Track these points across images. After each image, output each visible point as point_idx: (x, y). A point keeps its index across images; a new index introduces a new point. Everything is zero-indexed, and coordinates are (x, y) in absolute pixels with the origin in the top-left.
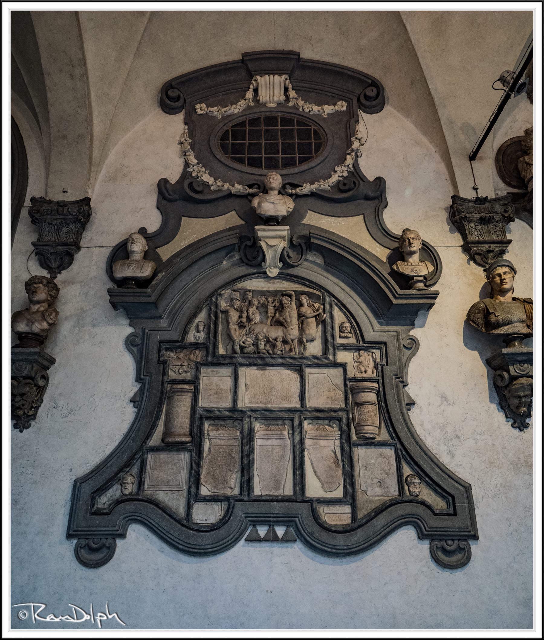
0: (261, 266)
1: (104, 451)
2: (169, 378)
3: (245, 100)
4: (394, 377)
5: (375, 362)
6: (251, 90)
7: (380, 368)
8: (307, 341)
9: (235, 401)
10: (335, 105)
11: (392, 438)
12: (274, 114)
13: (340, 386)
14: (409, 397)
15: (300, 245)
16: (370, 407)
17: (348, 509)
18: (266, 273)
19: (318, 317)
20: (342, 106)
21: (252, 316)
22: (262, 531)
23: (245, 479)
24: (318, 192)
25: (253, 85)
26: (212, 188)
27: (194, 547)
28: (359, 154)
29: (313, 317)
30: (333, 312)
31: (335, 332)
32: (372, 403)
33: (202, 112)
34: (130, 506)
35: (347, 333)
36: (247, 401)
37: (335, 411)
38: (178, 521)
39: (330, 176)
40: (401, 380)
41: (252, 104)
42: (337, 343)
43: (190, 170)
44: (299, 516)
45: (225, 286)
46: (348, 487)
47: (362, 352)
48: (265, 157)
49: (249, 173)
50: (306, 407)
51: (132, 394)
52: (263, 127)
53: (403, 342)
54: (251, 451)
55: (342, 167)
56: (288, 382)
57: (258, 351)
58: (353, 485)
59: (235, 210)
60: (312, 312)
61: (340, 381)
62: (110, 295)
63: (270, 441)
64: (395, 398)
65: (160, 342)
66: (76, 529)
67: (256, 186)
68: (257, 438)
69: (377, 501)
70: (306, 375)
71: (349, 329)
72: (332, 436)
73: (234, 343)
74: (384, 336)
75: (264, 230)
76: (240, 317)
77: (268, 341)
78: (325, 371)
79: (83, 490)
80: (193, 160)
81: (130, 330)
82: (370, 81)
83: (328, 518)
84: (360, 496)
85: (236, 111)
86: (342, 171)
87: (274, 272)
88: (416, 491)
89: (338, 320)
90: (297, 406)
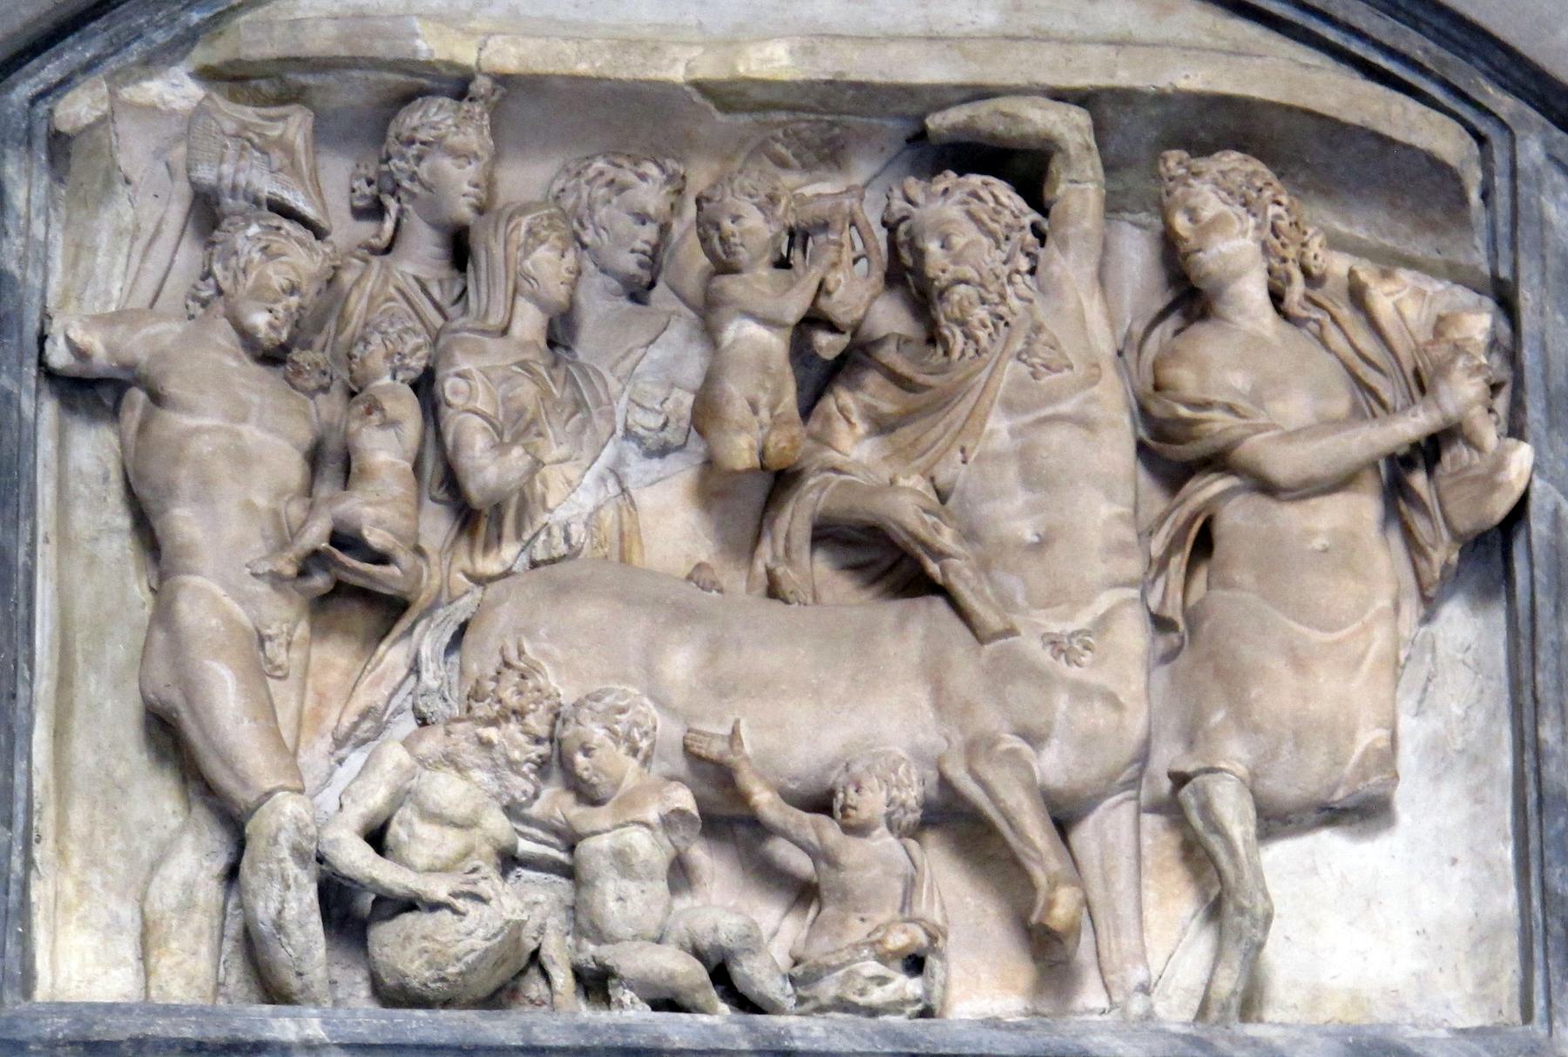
19: (1419, 480)
29: (1343, 482)
60: (1341, 405)
73: (240, 844)
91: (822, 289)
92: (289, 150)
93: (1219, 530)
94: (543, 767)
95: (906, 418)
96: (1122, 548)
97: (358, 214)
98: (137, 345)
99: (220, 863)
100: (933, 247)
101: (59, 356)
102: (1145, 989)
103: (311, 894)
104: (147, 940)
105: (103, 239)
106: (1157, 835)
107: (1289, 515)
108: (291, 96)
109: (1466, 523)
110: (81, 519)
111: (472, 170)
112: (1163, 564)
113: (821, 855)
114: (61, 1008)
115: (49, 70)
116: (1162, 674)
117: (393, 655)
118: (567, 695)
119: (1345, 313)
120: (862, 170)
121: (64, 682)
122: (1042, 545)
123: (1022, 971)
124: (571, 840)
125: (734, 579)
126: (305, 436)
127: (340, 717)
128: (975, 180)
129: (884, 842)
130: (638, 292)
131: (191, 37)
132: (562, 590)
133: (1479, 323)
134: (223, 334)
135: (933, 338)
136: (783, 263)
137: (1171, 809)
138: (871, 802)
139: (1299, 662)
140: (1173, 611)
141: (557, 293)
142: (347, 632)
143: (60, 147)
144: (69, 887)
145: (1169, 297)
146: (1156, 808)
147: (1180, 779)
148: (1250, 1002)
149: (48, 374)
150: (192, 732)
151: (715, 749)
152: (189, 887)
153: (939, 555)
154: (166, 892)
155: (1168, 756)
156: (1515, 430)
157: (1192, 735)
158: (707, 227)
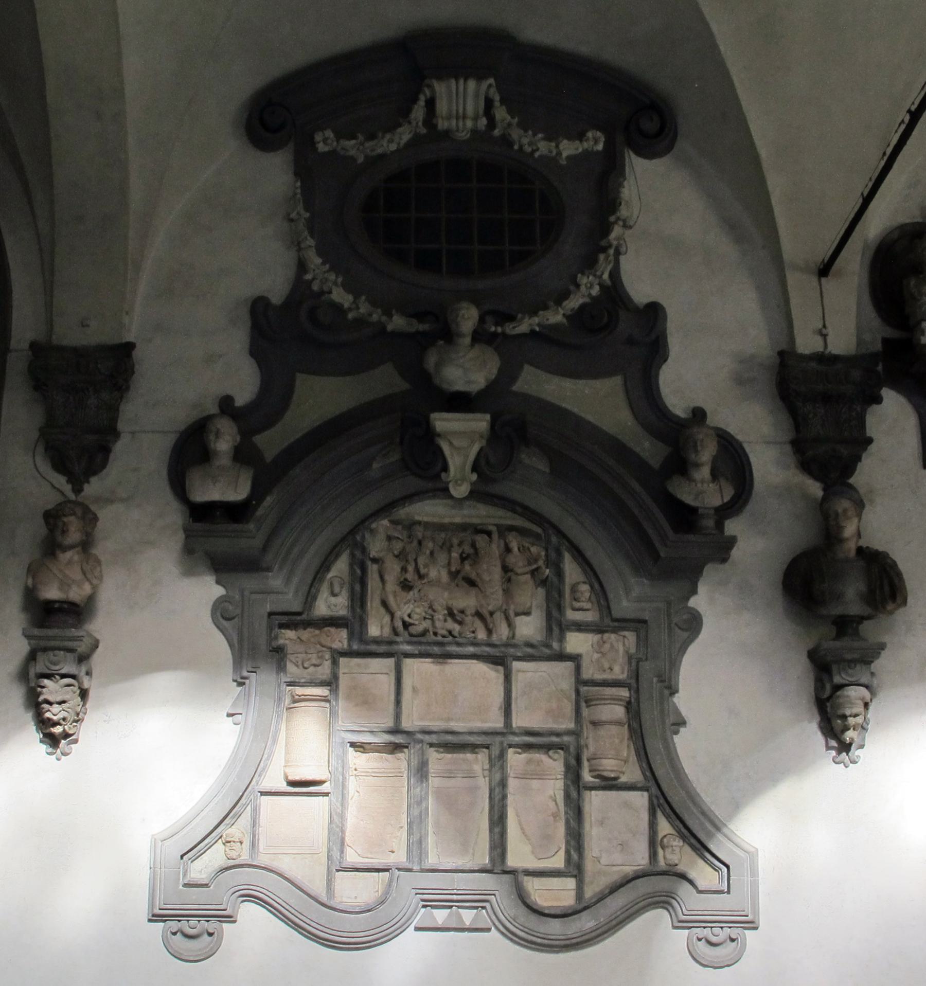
3: (410, 123)
5: (627, 652)
6: (422, 103)
7: (634, 664)
8: (517, 614)
9: (398, 716)
10: (581, 137)
14: (678, 712)
16: (614, 729)
17: (571, 883)
19: (536, 573)
20: (595, 141)
22: (440, 916)
23: (416, 838)
25: (425, 95)
26: (350, 316)
27: (339, 934)
28: (623, 249)
29: (527, 573)
30: (562, 566)
32: (619, 723)
33: (326, 149)
37: (558, 735)
40: (666, 684)
41: (423, 131)
43: (308, 277)
44: (496, 893)
45: (376, 514)
46: (572, 852)
47: (606, 635)
53: (675, 619)
55: (591, 278)
57: (435, 630)
60: (526, 563)
65: (270, 614)
68: (433, 775)
71: (587, 595)
72: (551, 775)
75: (444, 420)
76: (404, 570)
77: (451, 614)
78: (544, 666)
80: (314, 260)
81: (219, 591)
83: (539, 897)
84: (589, 866)
85: (393, 147)
86: (589, 285)
87: (460, 491)
88: (673, 858)
91: (463, 549)
98: (381, 555)
100: (477, 543)
101: (371, 556)
103: (401, 623)
104: (382, 627)
107: (520, 577)
114: (371, 637)
117: (411, 593)
122: (490, 580)
124: (433, 616)
127: (405, 601)
129: (470, 617)
134: (391, 554)
140: (505, 589)
150: (387, 603)
151: (450, 606)
155: (504, 607)
156: (547, 567)
157: (508, 604)
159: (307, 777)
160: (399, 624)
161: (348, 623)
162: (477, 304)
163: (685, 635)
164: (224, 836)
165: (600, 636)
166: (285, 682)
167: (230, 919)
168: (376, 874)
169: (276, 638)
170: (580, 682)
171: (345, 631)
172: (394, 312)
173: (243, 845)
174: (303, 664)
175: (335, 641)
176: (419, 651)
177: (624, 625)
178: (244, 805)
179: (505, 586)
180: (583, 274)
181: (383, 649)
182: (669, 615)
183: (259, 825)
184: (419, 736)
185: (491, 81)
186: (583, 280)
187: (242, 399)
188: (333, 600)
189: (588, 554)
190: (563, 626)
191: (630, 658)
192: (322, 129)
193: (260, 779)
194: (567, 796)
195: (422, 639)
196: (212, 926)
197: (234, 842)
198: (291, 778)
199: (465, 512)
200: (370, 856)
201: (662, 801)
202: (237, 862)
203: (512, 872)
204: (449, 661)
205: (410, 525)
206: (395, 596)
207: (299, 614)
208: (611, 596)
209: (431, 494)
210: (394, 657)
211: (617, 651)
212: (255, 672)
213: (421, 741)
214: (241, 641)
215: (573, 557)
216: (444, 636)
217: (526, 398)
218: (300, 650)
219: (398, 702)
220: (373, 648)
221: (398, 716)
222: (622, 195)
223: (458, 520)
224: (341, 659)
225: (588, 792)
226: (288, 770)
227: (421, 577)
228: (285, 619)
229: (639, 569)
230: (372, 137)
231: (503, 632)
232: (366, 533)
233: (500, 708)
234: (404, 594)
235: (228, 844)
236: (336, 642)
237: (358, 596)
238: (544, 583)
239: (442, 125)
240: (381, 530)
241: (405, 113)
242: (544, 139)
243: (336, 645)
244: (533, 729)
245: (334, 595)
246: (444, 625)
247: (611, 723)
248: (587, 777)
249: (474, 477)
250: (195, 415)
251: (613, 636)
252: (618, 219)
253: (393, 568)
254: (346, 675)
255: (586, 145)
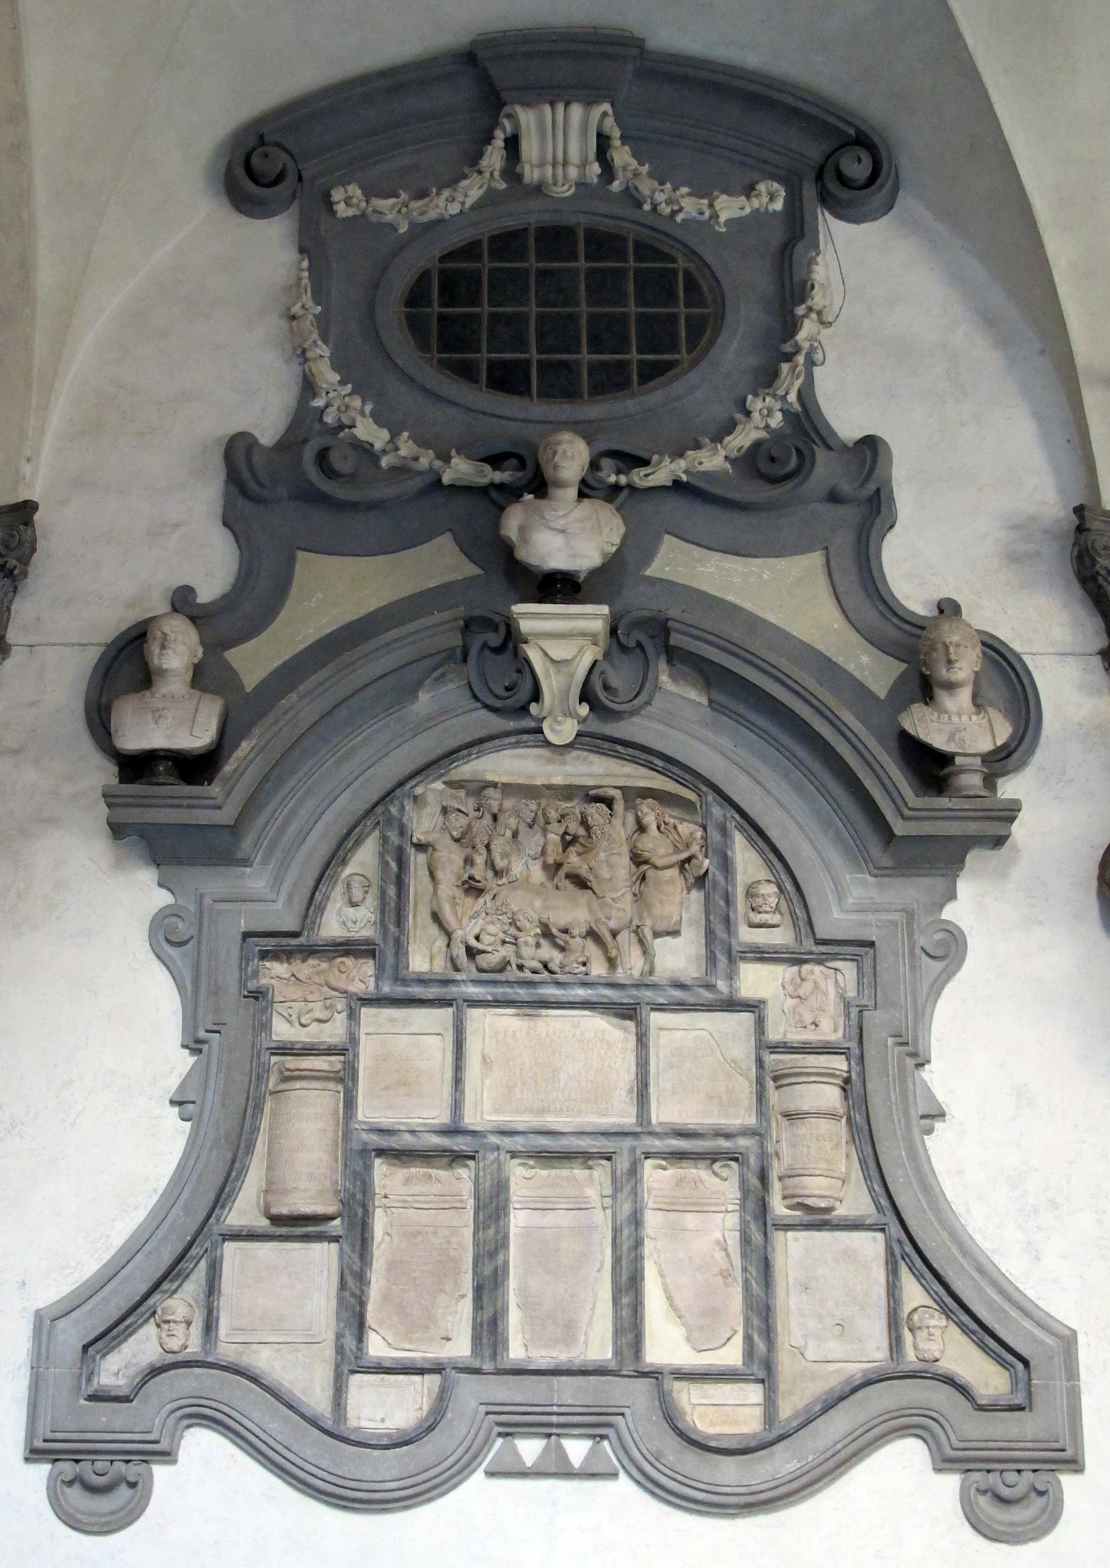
0: (528, 711)
1: (108, 1236)
2: (274, 1038)
3: (480, 172)
4: (890, 1041)
5: (842, 997)
6: (499, 142)
8: (657, 935)
9: (457, 1105)
10: (749, 190)
11: (879, 1208)
12: (567, 219)
13: (744, 1066)
14: (931, 1097)
15: (639, 645)
16: (824, 1126)
17: (754, 1393)
18: (542, 732)
19: (687, 866)
21: (500, 864)
22: (530, 1449)
23: (487, 1314)
24: (695, 482)
26: (384, 462)
27: (353, 1484)
28: (819, 356)
30: (729, 853)
31: (736, 911)
32: (833, 1116)
33: (351, 212)
34: (186, 1382)
35: (766, 912)
36: (487, 1104)
37: (728, 1136)
38: (314, 1422)
39: (730, 427)
40: (910, 1049)
41: (502, 186)
42: (740, 944)
43: (319, 402)
44: (627, 1411)
46: (756, 1338)
47: (806, 968)
48: (538, 362)
49: (493, 415)
50: (649, 1122)
51: (173, 1082)
52: (533, 263)
53: (922, 941)
54: (502, 1243)
55: (768, 399)
56: (602, 1052)
57: (520, 961)
58: (769, 1332)
59: (450, 530)
60: (671, 850)
61: (743, 1050)
62: (109, 806)
63: (551, 1215)
64: (890, 1100)
65: (246, 935)
66: (50, 1436)
67: (514, 462)
68: (517, 1206)
69: (832, 1378)
70: (652, 1032)
71: (773, 901)
72: (717, 1204)
73: (450, 939)
74: (867, 924)
76: (469, 861)
77: (547, 933)
78: (704, 1020)
79: (61, 1337)
80: (328, 377)
81: (164, 898)
82: (852, 132)
83: (701, 1417)
84: (785, 1363)
85: (454, 209)
86: (765, 412)
87: (561, 731)
88: (932, 1349)
89: (744, 873)
90: (626, 1120)
92: (461, 799)
93: (647, 875)
94: (510, 924)
95: (584, 853)
96: (627, 880)
97: (475, 810)
98: (430, 838)
99: (446, 943)
100: (589, 818)
101: (415, 840)
102: (631, 969)
105: (424, 815)
106: (634, 939)
107: (661, 873)
108: (462, 787)
109: (695, 875)
110: (420, 873)
111: (497, 803)
112: (635, 883)
113: (566, 942)
115: (413, 782)
116: (635, 905)
117: (481, 901)
118: (515, 909)
119: (672, 830)
120: (575, 802)
121: (416, 905)
122: (610, 880)
123: (606, 965)
125: (549, 885)
126: (463, 856)
127: (470, 913)
128: (598, 804)
129: (578, 940)
130: (531, 826)
131: (442, 775)
132: (515, 888)
133: (699, 834)
135: (590, 836)
136: (559, 821)
137: (636, 932)
138: (576, 932)
139: (661, 903)
140: (637, 892)
141: (515, 828)
142: (472, 895)
143: (416, 799)
144: (416, 947)
145: (636, 828)
146: (633, 932)
147: (638, 927)
148: (651, 972)
149: (412, 843)
150: (441, 917)
151: (545, 921)
152: (440, 948)
153: (590, 881)
154: (435, 949)
155: (636, 922)
156: (706, 856)
157: (641, 918)
158: (544, 815)
159: (302, 1209)
160: (460, 952)
161: (374, 950)
162: (589, 440)
163: (937, 966)
164: (159, 1312)
165: (795, 968)
166: (268, 1049)
167: (168, 1456)
168: (417, 1378)
169: (256, 974)
170: (764, 1046)
171: (371, 962)
172: (453, 452)
173: (191, 1328)
174: (299, 1019)
175: (353, 981)
176: (492, 994)
177: (836, 949)
178: (195, 1257)
179: (636, 889)
180: (756, 395)
181: (432, 992)
182: (911, 934)
183: (220, 1292)
184: (493, 1139)
185: (606, 107)
186: (756, 405)
187: (208, 592)
188: (351, 912)
189: (773, 834)
190: (734, 953)
191: (847, 1005)
192: (344, 185)
193: (222, 1214)
194: (745, 1240)
195: (500, 977)
196: (132, 1471)
197: (175, 1322)
198: (274, 1210)
199: (569, 768)
200: (407, 1346)
201: (909, 1248)
202: (179, 1358)
203: (654, 1374)
204: (544, 1012)
205: (479, 788)
206: (454, 905)
207: (295, 935)
208: (812, 902)
209: (513, 739)
210: (452, 1005)
211: (825, 994)
212: (219, 1032)
213: (498, 1148)
214: (196, 981)
215: (749, 839)
216: (535, 972)
217: (670, 587)
218: (294, 997)
219: (458, 1081)
220: (417, 991)
221: (457, 1105)
222: (815, 276)
223: (558, 780)
224: (364, 1010)
225: (781, 1234)
226: (270, 1198)
227: (498, 873)
228: (270, 943)
229: (859, 858)
230: (423, 194)
231: (633, 964)
232: (405, 803)
233: (631, 1091)
234: (469, 901)
235: (166, 1326)
236: (354, 983)
237: (393, 905)
238: (701, 881)
239: (530, 174)
240: (431, 798)
241: (474, 159)
242: (689, 194)
243: (356, 988)
244: (684, 1127)
245: (354, 905)
246: (535, 952)
247: (818, 1114)
248: (779, 1208)
249: (584, 710)
250: (133, 617)
251: (817, 969)
252: (810, 309)
253: (450, 859)
254: (370, 1037)
255: (756, 203)
